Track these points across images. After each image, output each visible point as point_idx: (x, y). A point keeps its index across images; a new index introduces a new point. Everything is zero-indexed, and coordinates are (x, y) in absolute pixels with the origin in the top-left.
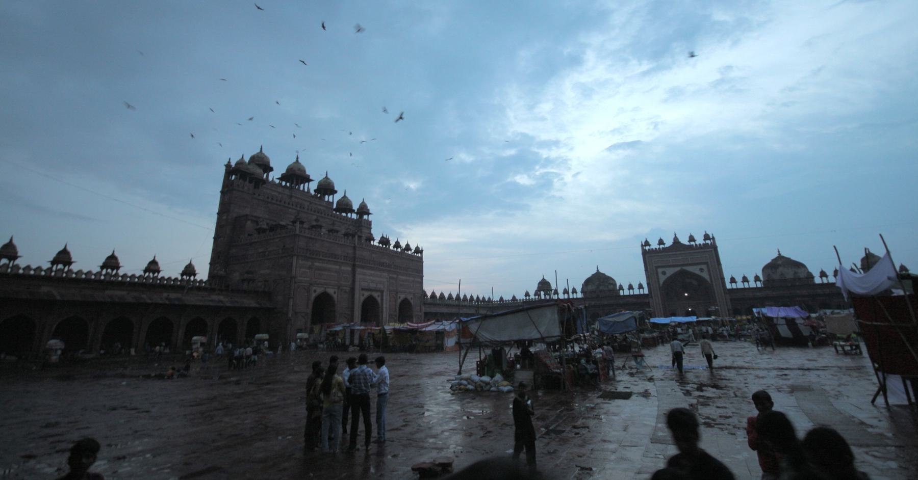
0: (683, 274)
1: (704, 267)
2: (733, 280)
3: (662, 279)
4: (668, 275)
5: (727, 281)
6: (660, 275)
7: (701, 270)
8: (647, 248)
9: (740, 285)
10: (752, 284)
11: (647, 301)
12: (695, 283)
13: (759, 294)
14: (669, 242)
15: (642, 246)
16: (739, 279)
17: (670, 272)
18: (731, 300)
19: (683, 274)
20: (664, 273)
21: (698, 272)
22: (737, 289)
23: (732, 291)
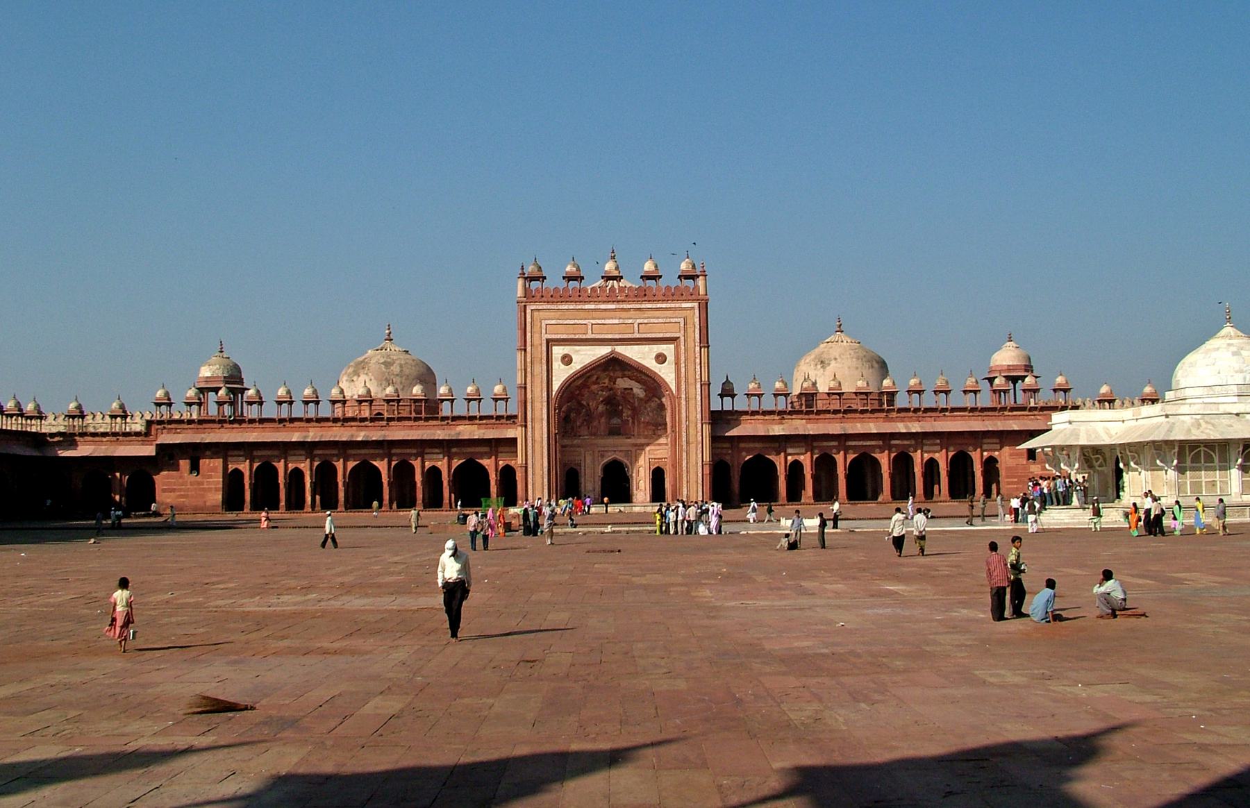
0: (614, 364)
1: (668, 350)
2: (728, 391)
3: (561, 374)
4: (577, 365)
6: (557, 365)
7: (661, 358)
8: (535, 285)
11: (510, 433)
12: (638, 390)
17: (584, 356)
18: (715, 439)
19: (614, 364)
20: (567, 360)
21: (650, 363)
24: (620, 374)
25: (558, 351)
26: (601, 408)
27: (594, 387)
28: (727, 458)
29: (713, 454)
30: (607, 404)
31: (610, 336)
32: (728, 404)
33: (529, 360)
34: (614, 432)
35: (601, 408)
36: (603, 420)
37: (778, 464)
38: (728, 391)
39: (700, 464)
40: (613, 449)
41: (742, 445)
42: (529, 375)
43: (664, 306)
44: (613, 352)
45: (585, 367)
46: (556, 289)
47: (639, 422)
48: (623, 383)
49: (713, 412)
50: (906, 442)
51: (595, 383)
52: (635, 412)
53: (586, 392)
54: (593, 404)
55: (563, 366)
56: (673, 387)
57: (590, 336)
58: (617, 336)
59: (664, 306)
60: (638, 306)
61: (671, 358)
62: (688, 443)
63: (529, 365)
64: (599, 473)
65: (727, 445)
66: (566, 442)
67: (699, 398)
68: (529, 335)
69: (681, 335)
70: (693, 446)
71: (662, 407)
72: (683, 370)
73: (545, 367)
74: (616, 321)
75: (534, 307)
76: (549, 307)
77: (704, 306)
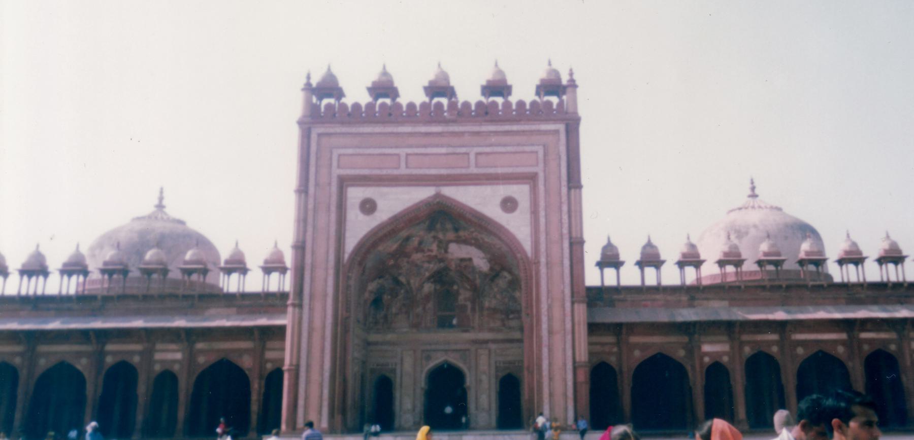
2: (610, 259)
3: (359, 227)
5: (592, 254)
7: (509, 204)
9: (630, 276)
10: (670, 276)
13: (687, 315)
14: (412, 93)
15: (309, 88)
16: (630, 254)
17: (395, 202)
18: (593, 328)
20: (368, 207)
21: (492, 211)
22: (617, 290)
23: (598, 297)
24: (451, 235)
25: (356, 194)
26: (428, 288)
27: (417, 257)
28: (613, 360)
29: (591, 354)
30: (435, 282)
31: (433, 172)
32: (610, 278)
33: (311, 206)
34: (444, 323)
35: (428, 288)
36: (430, 305)
37: (689, 368)
38: (610, 259)
39: (570, 366)
40: (446, 345)
41: (634, 339)
42: (310, 229)
43: (515, 128)
44: (438, 195)
45: (395, 219)
46: (356, 106)
47: (482, 309)
48: (457, 251)
49: (590, 289)
50: (883, 335)
51: (419, 249)
52: (477, 293)
53: (404, 263)
54: (414, 282)
55: (361, 216)
56: (527, 246)
57: (403, 171)
58: (444, 172)
59: (515, 128)
60: (476, 129)
61: (524, 202)
62: (551, 332)
63: (310, 213)
64: (422, 383)
65: (611, 339)
66: (373, 337)
67: (567, 263)
68: (312, 170)
69: (539, 170)
70: (557, 338)
71: (514, 283)
72: (542, 221)
73: (333, 217)
74: (443, 150)
75: (321, 130)
76: (345, 129)
77: (572, 125)
